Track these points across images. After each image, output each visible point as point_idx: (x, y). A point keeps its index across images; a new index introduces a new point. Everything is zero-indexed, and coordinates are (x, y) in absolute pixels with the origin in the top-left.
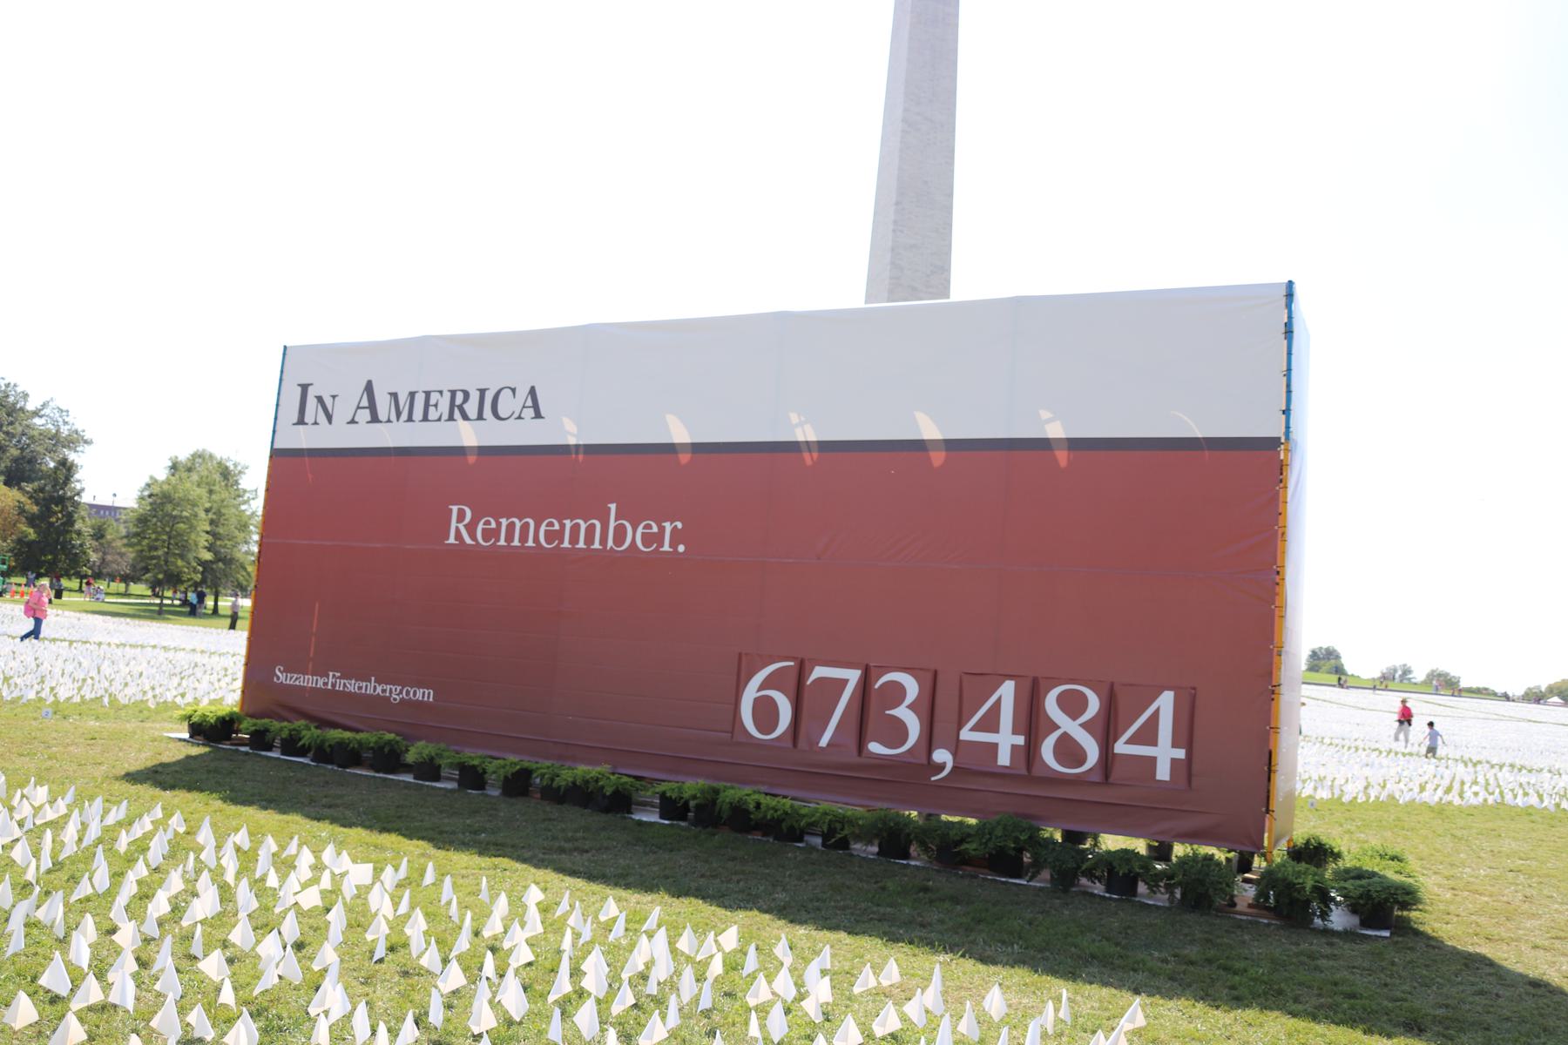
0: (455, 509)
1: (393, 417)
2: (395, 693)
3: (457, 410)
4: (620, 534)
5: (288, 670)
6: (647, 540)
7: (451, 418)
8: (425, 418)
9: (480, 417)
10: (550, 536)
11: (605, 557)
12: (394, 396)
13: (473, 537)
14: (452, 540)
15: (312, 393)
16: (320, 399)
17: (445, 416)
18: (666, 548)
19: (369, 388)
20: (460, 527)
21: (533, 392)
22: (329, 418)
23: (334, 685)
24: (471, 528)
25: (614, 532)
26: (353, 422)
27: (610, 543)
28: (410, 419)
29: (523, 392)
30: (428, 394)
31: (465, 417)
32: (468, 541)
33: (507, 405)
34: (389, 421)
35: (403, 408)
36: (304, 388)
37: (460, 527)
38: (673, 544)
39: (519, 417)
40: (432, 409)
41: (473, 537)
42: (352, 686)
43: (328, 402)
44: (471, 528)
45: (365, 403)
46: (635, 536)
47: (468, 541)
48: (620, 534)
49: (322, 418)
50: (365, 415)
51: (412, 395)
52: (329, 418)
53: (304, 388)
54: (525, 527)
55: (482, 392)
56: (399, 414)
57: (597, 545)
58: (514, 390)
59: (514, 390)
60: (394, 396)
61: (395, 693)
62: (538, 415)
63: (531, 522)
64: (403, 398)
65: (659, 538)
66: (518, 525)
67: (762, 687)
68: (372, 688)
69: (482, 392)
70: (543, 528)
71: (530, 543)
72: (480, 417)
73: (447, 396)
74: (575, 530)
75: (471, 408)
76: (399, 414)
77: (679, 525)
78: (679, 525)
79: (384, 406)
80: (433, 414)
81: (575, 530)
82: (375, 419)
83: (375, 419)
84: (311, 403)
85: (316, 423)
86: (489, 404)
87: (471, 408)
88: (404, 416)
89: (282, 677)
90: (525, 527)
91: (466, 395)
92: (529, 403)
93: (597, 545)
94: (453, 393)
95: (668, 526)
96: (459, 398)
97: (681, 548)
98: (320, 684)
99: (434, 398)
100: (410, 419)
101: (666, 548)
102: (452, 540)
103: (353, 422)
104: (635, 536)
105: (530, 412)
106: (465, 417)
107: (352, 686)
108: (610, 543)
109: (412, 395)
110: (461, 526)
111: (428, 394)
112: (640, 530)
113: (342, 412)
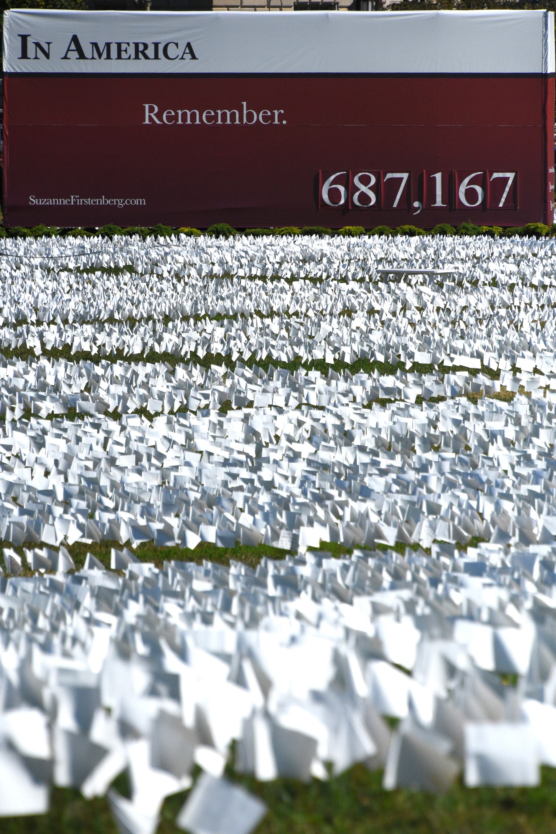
0: (147, 106)
1: (96, 55)
2: (120, 203)
3: (140, 51)
4: (250, 117)
5: (38, 197)
6: (265, 118)
7: (137, 57)
8: (119, 57)
9: (156, 57)
10: (209, 118)
11: (242, 126)
12: (95, 45)
13: (161, 119)
14: (147, 122)
15: (30, 41)
16: (38, 45)
17: (133, 56)
18: (276, 122)
19: (75, 39)
20: (150, 114)
21: (189, 45)
22: (47, 56)
23: (75, 203)
24: (159, 116)
25: (244, 115)
26: (65, 58)
27: (245, 121)
28: (109, 57)
30: (119, 45)
31: (146, 57)
32: (158, 122)
33: (172, 51)
34: (93, 58)
35: (102, 51)
36: (24, 38)
37: (150, 114)
38: (280, 120)
39: (182, 58)
40: (123, 53)
41: (161, 119)
42: (89, 202)
43: (45, 47)
45: (73, 47)
46: (259, 117)
47: (158, 122)
48: (250, 117)
50: (76, 54)
51: (108, 45)
52: (47, 56)
53: (24, 38)
55: (156, 45)
56: (100, 55)
57: (237, 122)
58: (177, 44)
59: (177, 44)
60: (95, 45)
61: (120, 203)
62: (194, 57)
63: (197, 112)
64: (101, 47)
65: (272, 117)
66: (189, 113)
67: (332, 184)
68: (103, 201)
69: (156, 45)
70: (204, 115)
71: (198, 122)
72: (156, 57)
73: (133, 46)
74: (224, 116)
75: (150, 52)
76: (100, 55)
77: (282, 112)
78: (282, 112)
79: (88, 50)
80: (123, 55)
81: (224, 116)
82: (82, 56)
83: (82, 56)
84: (31, 48)
85: (36, 58)
86: (162, 51)
87: (150, 52)
88: (104, 55)
89: (34, 201)
91: (146, 46)
92: (187, 51)
93: (237, 122)
94: (137, 45)
95: (276, 113)
96: (141, 48)
97: (284, 122)
98: (65, 202)
99: (123, 47)
100: (109, 57)
101: (276, 122)
102: (147, 122)
103: (65, 58)
104: (259, 117)
105: (189, 56)
106: (146, 57)
107: (89, 202)
108: (245, 121)
109: (108, 45)
110: (152, 115)
111: (119, 45)
112: (261, 115)
113: (57, 51)
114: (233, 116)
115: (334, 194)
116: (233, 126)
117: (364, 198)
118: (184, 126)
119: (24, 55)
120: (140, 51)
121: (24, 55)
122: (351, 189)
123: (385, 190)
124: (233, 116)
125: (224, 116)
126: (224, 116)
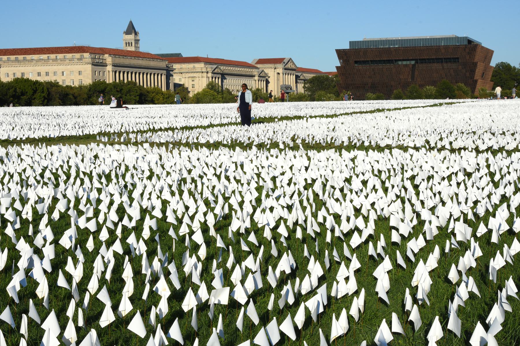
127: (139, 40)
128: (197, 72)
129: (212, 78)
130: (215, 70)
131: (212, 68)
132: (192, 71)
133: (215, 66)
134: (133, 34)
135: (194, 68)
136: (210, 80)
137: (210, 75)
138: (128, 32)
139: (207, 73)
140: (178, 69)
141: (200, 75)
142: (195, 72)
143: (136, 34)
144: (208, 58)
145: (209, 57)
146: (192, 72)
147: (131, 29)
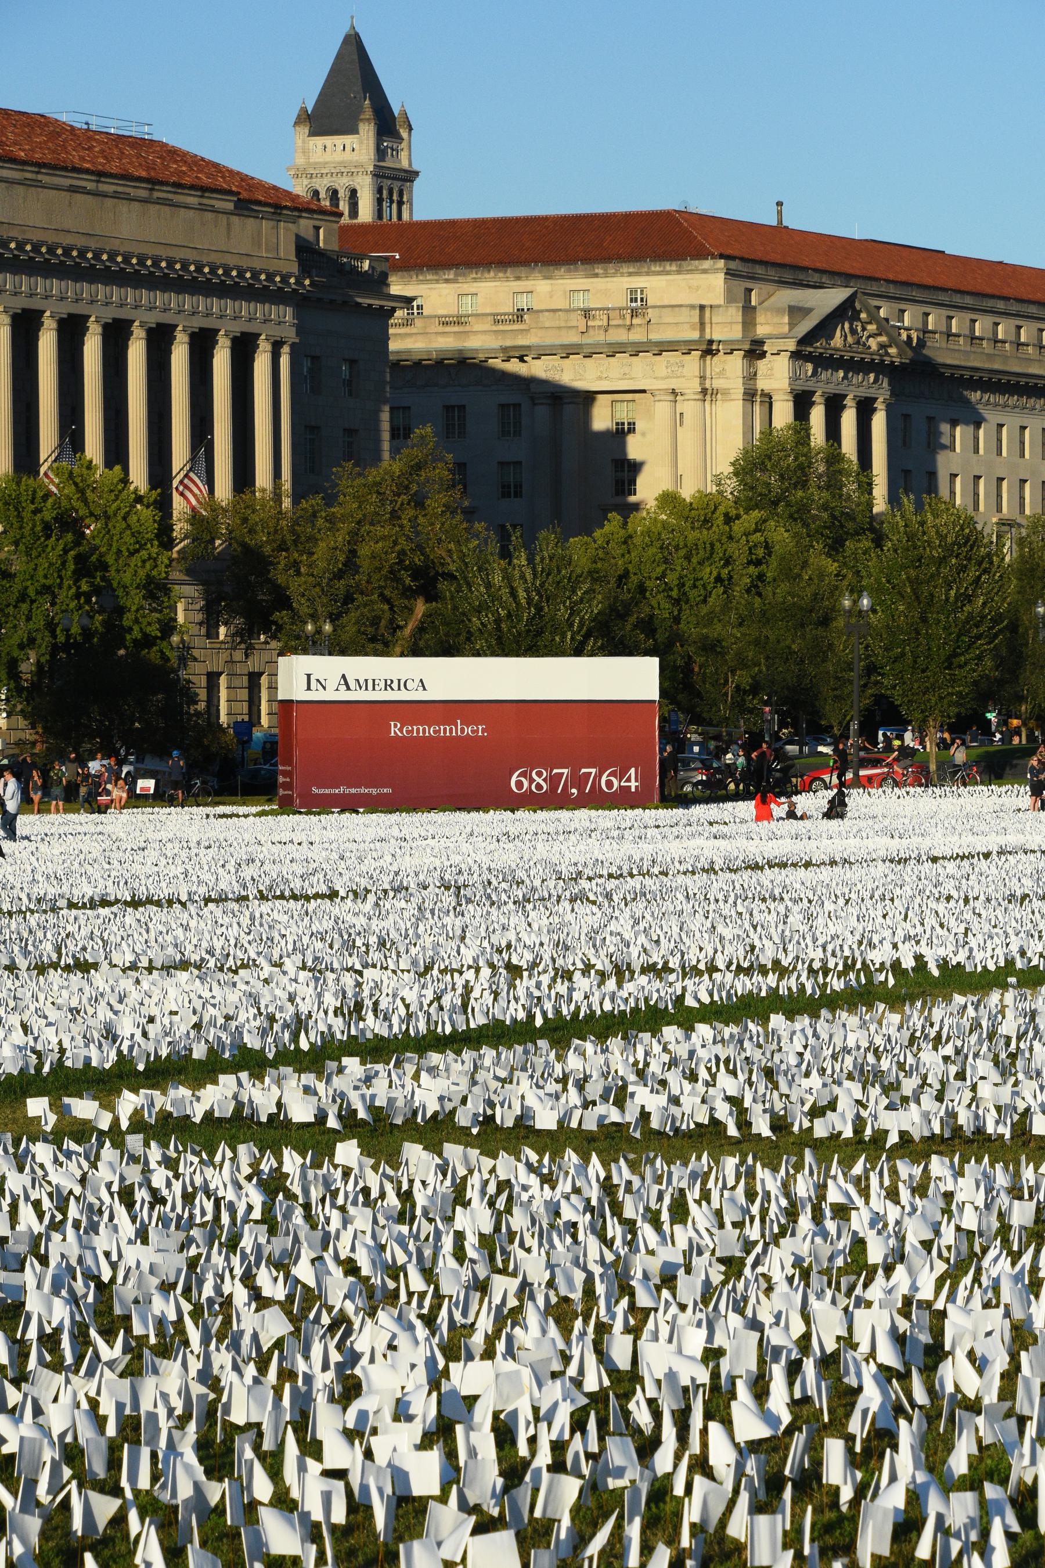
2: (374, 791)
3: (388, 685)
4: (463, 730)
10: (435, 732)
19: (344, 676)
20: (395, 729)
24: (401, 730)
29: (417, 681)
36: (309, 676)
37: (395, 729)
42: (353, 791)
44: (401, 730)
46: (468, 731)
48: (463, 730)
49: (320, 687)
53: (309, 676)
54: (424, 730)
61: (374, 791)
75: (395, 686)
79: (352, 684)
82: (348, 688)
83: (348, 688)
84: (314, 684)
86: (403, 685)
87: (395, 686)
90: (424, 730)
104: (468, 731)
107: (353, 791)
113: (331, 685)
114: (451, 730)
115: (519, 785)
116: (451, 736)
117: (539, 787)
118: (418, 737)
119: (309, 688)
120: (388, 685)
121: (309, 688)
122: (532, 780)
123: (554, 781)
124: (451, 730)
125: (445, 730)
126: (445, 730)
127: (410, 176)
128: (662, 348)
129: (802, 403)
130: (825, 328)
131: (796, 312)
132: (619, 336)
133: (833, 297)
134: (367, 131)
135: (638, 306)
136: (783, 414)
137: (777, 374)
138: (325, 119)
139: (755, 351)
140: (497, 319)
141: (687, 370)
142: (637, 350)
143: (388, 126)
144: (781, 230)
145: (791, 221)
146: (614, 350)
147: (354, 94)
